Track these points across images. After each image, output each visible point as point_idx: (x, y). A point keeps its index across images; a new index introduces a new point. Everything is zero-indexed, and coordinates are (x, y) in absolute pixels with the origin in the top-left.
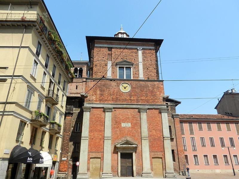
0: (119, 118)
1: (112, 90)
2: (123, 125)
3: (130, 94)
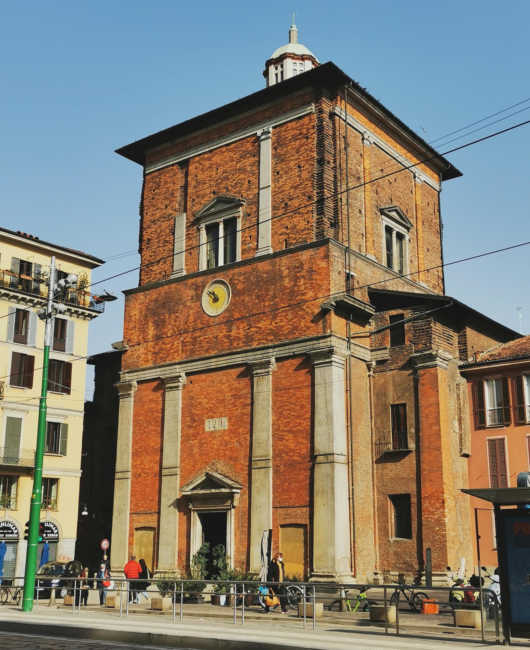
0: (199, 403)
1: (182, 317)
2: (210, 425)
3: (228, 320)
